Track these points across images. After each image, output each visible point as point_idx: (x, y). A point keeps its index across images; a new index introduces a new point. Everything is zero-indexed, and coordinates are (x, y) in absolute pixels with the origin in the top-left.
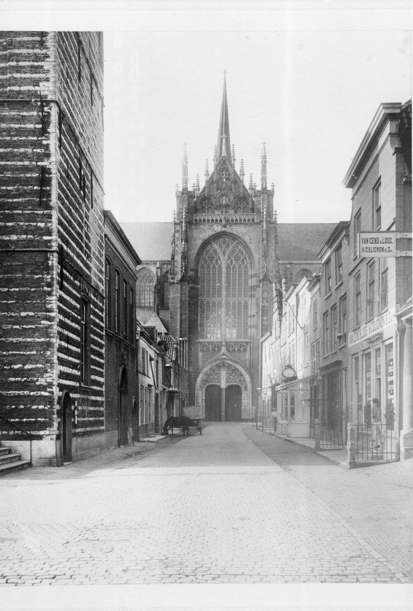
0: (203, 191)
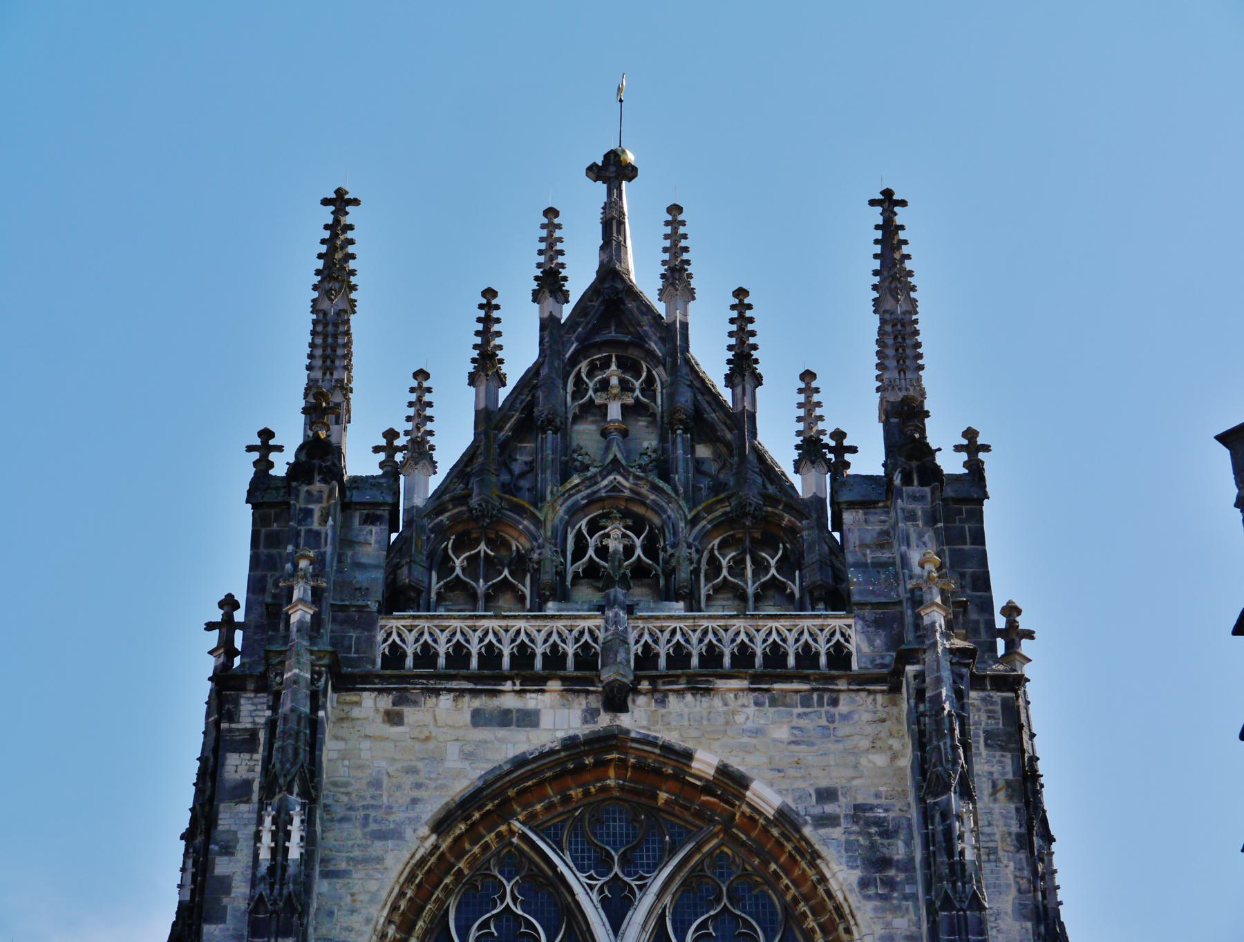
0: (462, 470)
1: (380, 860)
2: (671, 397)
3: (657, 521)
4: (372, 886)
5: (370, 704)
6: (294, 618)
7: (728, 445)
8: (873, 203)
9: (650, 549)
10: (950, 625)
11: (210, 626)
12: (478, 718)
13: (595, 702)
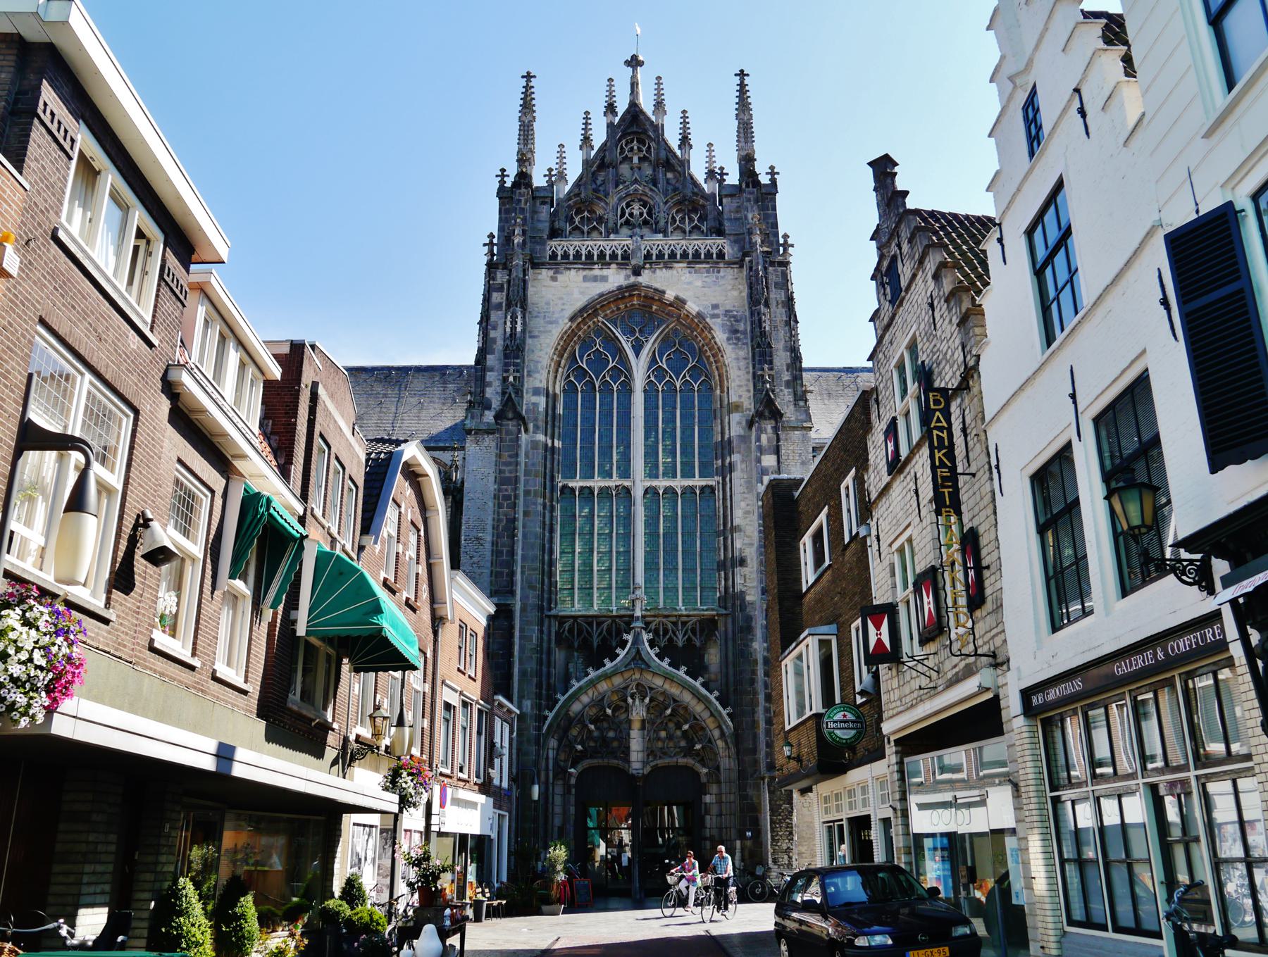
0: (578, 184)
1: (550, 331)
2: (657, 154)
3: (652, 203)
4: (548, 341)
5: (545, 274)
6: (516, 242)
7: (679, 173)
8: (736, 75)
9: (650, 214)
10: (762, 242)
11: (485, 245)
12: (585, 279)
13: (629, 272)
